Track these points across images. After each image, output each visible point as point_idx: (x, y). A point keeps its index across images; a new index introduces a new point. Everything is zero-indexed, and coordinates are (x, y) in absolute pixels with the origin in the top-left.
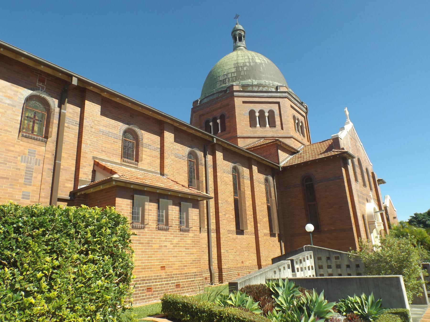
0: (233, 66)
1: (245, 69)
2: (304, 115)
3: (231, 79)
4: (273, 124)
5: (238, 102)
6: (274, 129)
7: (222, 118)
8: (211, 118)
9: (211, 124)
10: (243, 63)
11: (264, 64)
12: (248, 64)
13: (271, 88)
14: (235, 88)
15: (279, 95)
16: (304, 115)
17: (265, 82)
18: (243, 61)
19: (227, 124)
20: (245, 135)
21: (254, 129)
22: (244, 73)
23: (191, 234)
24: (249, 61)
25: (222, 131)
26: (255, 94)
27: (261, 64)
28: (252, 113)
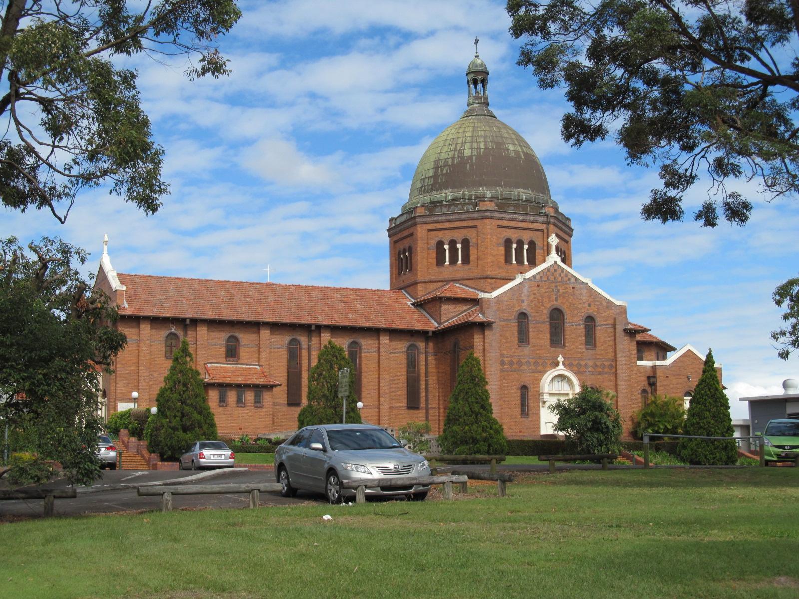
0: (432, 166)
1: (445, 171)
2: (544, 227)
3: (427, 187)
4: (466, 259)
5: (421, 231)
6: (466, 267)
7: (410, 249)
8: (402, 248)
9: (402, 256)
10: (445, 159)
11: (474, 158)
12: (450, 161)
13: (468, 206)
14: (420, 211)
15: (476, 215)
16: (544, 227)
17: (464, 195)
18: (446, 157)
19: (413, 261)
20: (427, 279)
21: (441, 269)
22: (443, 179)
23: (264, 410)
24: (454, 155)
25: (409, 270)
26: (444, 218)
27: (471, 157)
28: (440, 244)
